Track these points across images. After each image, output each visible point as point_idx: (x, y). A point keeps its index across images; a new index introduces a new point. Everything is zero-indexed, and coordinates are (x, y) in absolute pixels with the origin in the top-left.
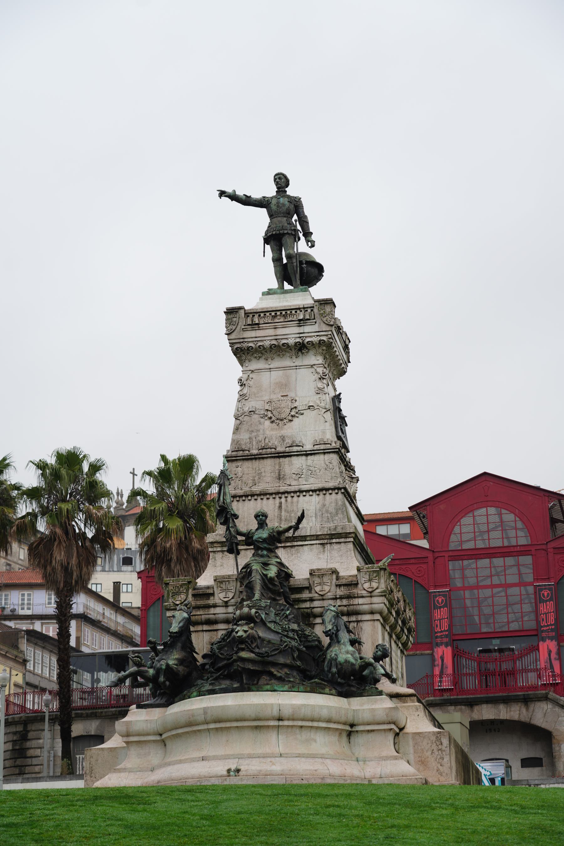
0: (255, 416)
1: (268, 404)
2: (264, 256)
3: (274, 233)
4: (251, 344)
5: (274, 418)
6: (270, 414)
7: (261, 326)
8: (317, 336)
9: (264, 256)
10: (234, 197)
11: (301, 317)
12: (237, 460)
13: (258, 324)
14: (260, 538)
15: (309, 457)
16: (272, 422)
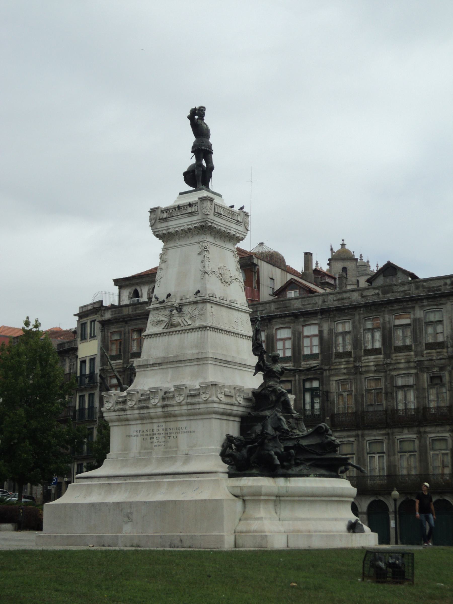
0: (214, 275)
1: (220, 270)
2: (191, 158)
3: (207, 149)
4: (215, 226)
5: (223, 281)
6: (222, 278)
7: (222, 216)
8: (242, 234)
9: (191, 158)
11: (239, 220)
12: (212, 303)
13: (221, 214)
14: (278, 370)
15: (240, 313)
16: (222, 282)
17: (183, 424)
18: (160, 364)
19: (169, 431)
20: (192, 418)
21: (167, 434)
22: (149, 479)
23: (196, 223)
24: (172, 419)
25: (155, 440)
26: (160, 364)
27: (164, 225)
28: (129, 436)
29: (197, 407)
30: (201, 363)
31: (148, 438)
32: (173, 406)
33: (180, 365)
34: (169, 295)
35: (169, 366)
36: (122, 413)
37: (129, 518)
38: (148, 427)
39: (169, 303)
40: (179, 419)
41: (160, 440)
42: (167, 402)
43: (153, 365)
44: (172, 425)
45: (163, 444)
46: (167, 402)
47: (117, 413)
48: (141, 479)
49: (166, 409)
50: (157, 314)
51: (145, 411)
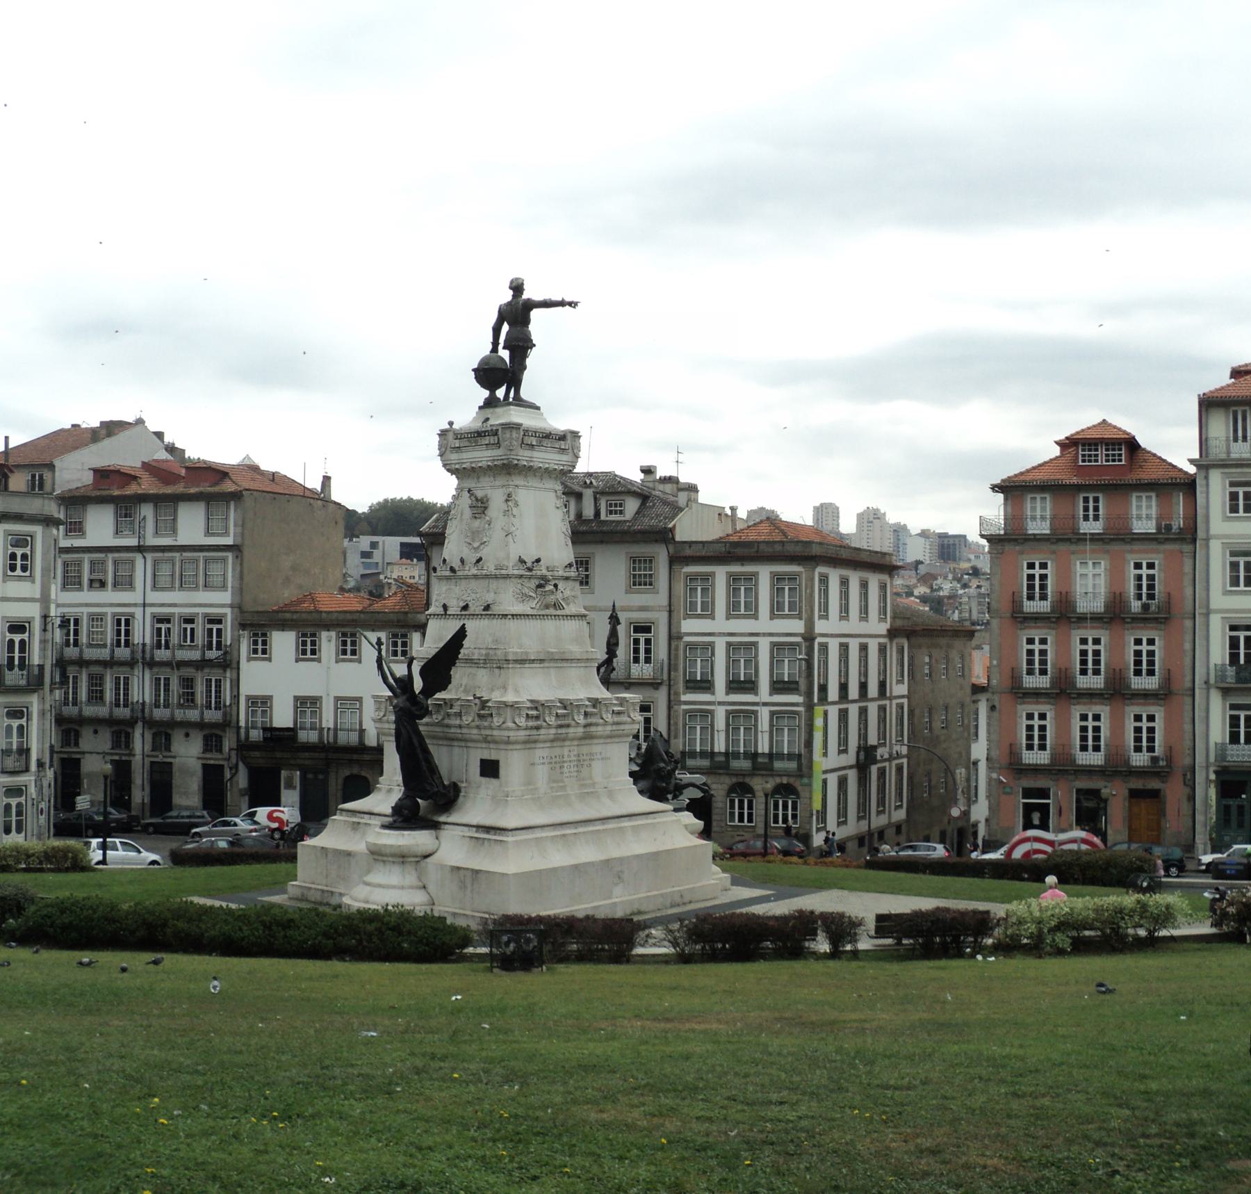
10: (562, 304)
17: (597, 748)
18: (542, 661)
19: (582, 758)
20: (609, 740)
21: (580, 762)
22: (603, 824)
23: (563, 465)
24: (587, 741)
25: (565, 770)
26: (542, 661)
27: (528, 453)
28: (533, 764)
29: (622, 727)
30: (588, 664)
31: (558, 765)
32: (597, 725)
33: (565, 665)
34: (538, 561)
35: (552, 665)
36: (534, 732)
37: (619, 877)
38: (557, 751)
39: (539, 573)
40: (596, 741)
41: (572, 769)
42: (589, 720)
43: (533, 661)
44: (585, 750)
45: (575, 774)
46: (589, 720)
47: (528, 732)
48: (594, 825)
49: (588, 729)
50: (520, 586)
51: (563, 731)
